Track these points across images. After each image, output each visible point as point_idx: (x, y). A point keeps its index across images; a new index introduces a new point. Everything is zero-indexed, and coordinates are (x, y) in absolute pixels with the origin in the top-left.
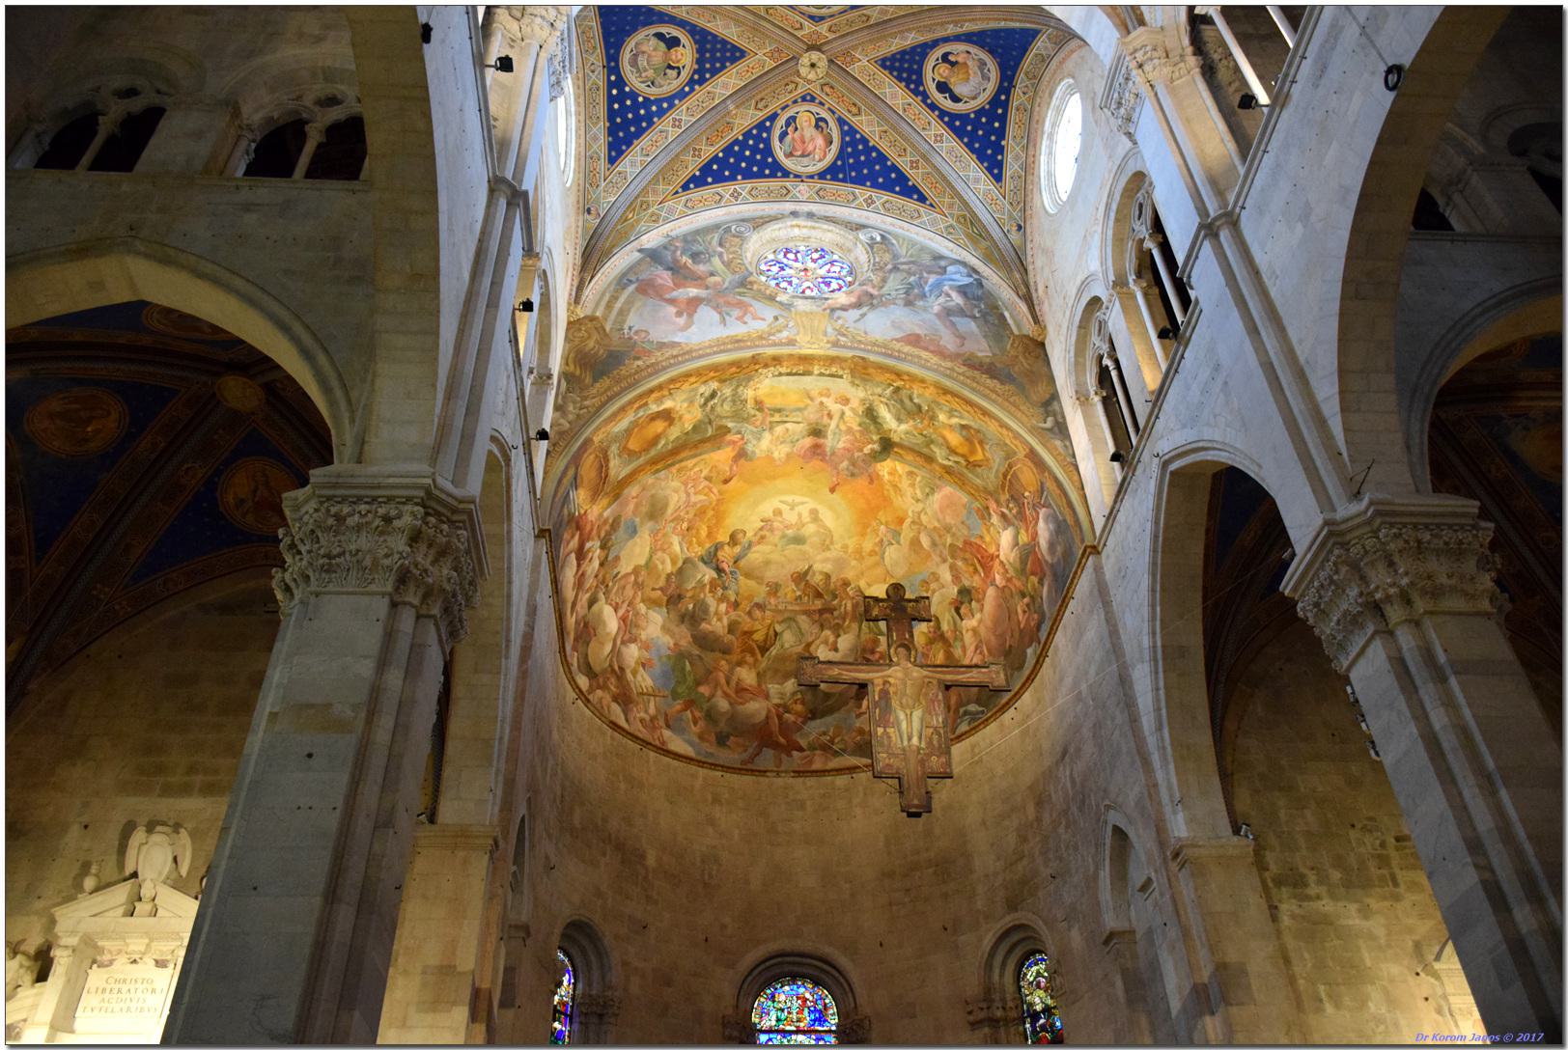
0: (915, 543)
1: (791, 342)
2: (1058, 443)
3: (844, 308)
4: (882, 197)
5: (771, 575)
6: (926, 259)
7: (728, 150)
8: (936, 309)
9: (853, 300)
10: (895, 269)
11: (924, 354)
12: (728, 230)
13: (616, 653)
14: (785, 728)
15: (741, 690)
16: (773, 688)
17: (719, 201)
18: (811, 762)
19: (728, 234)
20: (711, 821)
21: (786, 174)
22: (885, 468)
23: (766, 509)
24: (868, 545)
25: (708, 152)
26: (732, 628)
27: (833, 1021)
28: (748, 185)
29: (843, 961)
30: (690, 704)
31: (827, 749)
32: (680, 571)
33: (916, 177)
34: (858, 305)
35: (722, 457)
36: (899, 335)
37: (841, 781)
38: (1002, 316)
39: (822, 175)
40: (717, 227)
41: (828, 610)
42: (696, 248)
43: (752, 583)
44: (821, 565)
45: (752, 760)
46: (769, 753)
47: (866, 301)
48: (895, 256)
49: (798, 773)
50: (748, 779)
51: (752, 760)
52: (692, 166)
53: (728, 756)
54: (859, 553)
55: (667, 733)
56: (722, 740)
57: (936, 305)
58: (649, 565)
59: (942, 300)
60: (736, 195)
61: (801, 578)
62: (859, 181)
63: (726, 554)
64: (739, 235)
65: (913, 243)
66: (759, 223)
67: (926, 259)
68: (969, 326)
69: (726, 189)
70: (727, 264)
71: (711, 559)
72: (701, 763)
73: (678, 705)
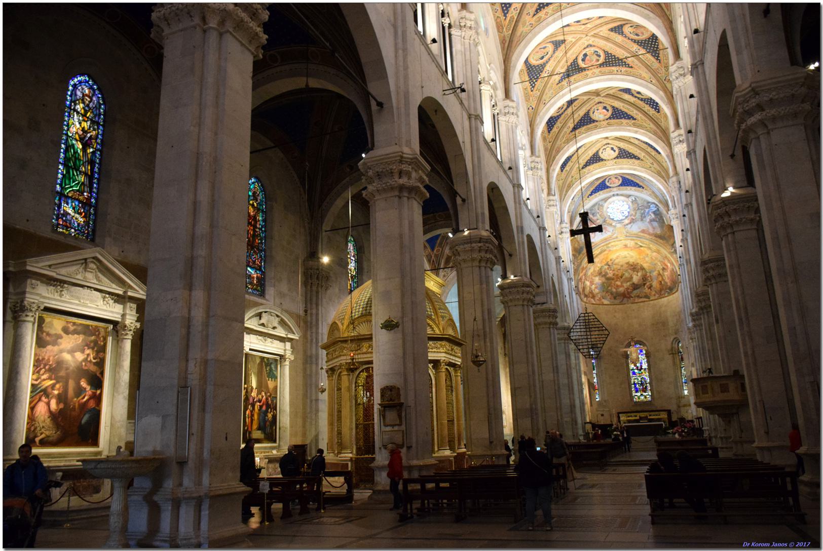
0: (652, 258)
1: (617, 238)
2: (675, 255)
3: (627, 225)
4: (633, 188)
5: (621, 264)
6: (645, 204)
7: (596, 187)
8: (648, 220)
9: (629, 221)
10: (638, 209)
11: (646, 235)
12: (599, 204)
13: (590, 288)
14: (628, 293)
15: (617, 286)
16: (625, 285)
17: (596, 196)
18: (634, 300)
19: (598, 205)
20: (615, 316)
21: (610, 187)
22: (642, 248)
23: (617, 254)
24: (641, 257)
25: (592, 189)
26: (614, 275)
27: (644, 352)
28: (602, 191)
29: (645, 342)
30: (607, 292)
31: (638, 297)
32: (601, 269)
33: (641, 184)
34: (630, 223)
35: (606, 252)
36: (640, 230)
37: (642, 304)
38: (663, 220)
39: (619, 186)
40: (597, 203)
41: (634, 268)
42: (593, 212)
43: (617, 266)
44: (631, 261)
45: (622, 301)
46: (625, 299)
47: (633, 221)
48: (638, 205)
49: (632, 303)
50: (621, 306)
51: (622, 301)
52: (589, 193)
53: (617, 301)
54: (640, 258)
55: (603, 300)
56: (615, 298)
57: (648, 219)
58: (594, 271)
59: (650, 217)
60: (599, 194)
61: (628, 263)
62: (628, 185)
63: (610, 263)
64: (602, 206)
65: (642, 199)
66: (605, 200)
67: (645, 204)
68: (655, 224)
69: (597, 194)
70: (600, 216)
71: (607, 264)
72: (611, 305)
73: (604, 293)
